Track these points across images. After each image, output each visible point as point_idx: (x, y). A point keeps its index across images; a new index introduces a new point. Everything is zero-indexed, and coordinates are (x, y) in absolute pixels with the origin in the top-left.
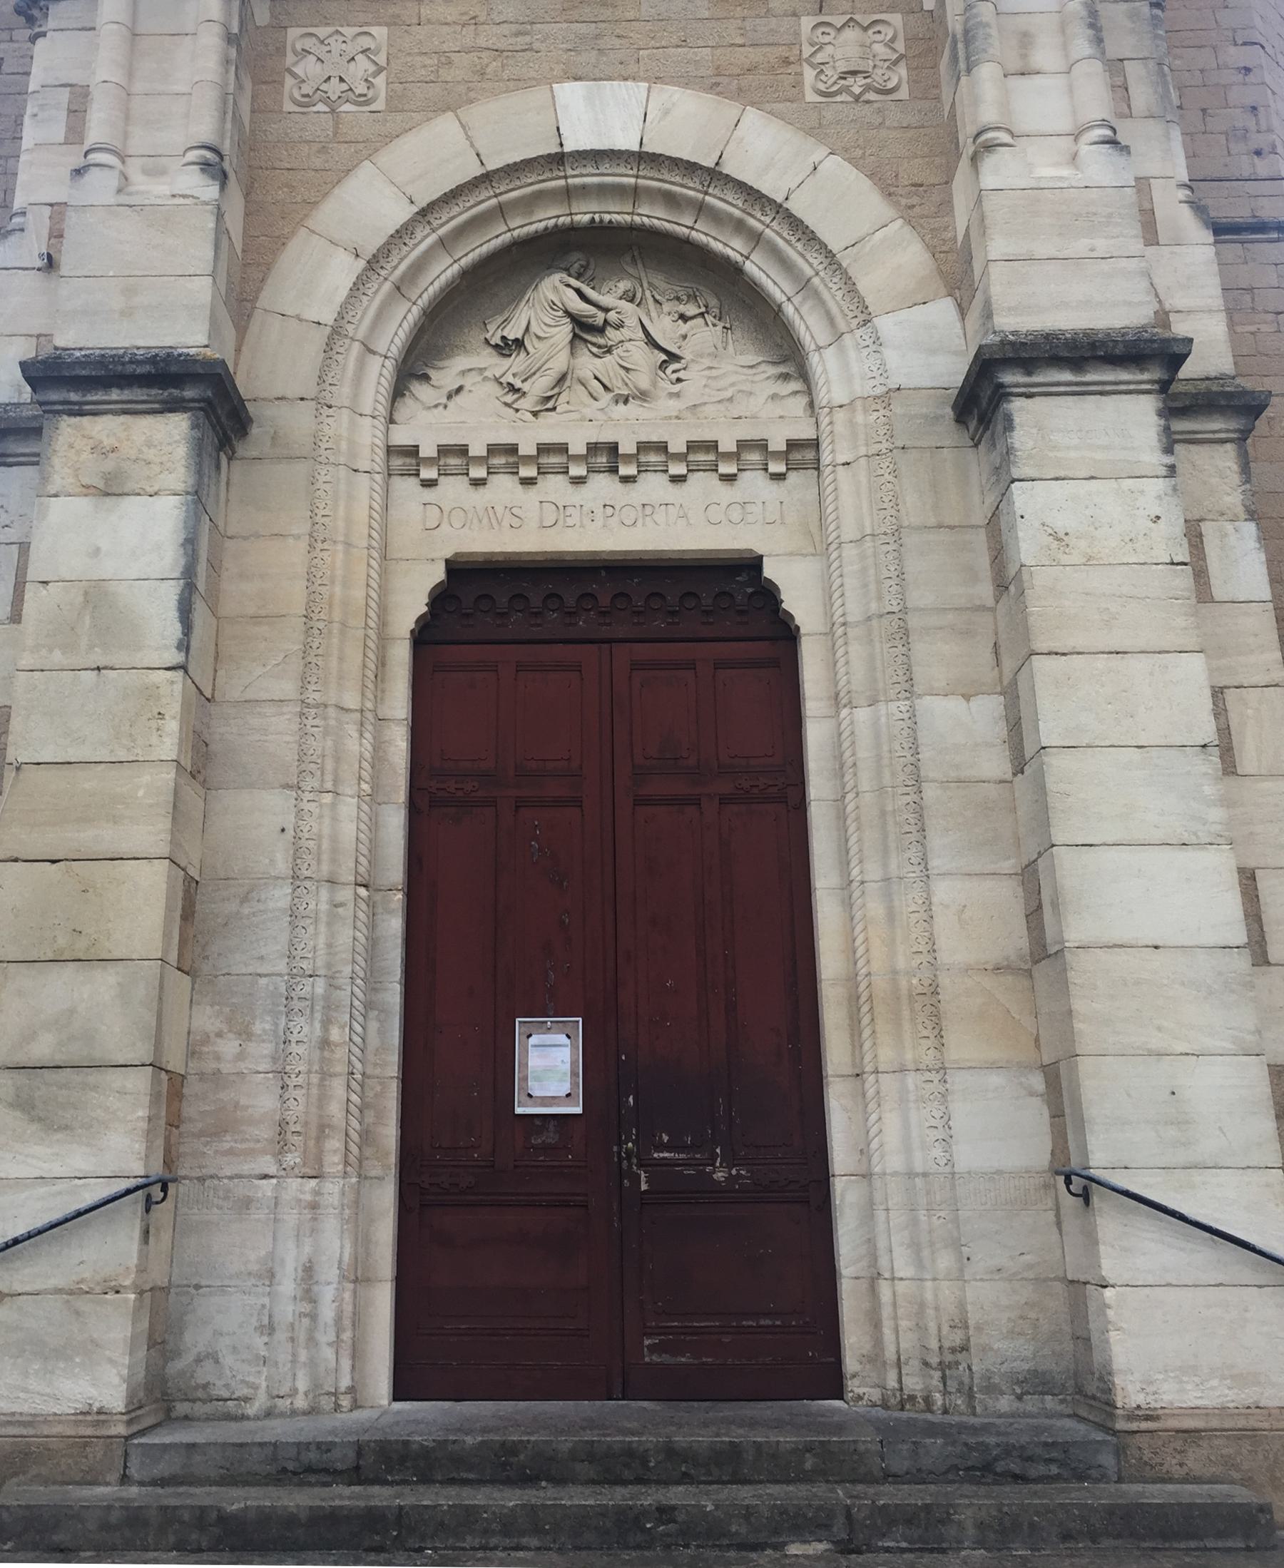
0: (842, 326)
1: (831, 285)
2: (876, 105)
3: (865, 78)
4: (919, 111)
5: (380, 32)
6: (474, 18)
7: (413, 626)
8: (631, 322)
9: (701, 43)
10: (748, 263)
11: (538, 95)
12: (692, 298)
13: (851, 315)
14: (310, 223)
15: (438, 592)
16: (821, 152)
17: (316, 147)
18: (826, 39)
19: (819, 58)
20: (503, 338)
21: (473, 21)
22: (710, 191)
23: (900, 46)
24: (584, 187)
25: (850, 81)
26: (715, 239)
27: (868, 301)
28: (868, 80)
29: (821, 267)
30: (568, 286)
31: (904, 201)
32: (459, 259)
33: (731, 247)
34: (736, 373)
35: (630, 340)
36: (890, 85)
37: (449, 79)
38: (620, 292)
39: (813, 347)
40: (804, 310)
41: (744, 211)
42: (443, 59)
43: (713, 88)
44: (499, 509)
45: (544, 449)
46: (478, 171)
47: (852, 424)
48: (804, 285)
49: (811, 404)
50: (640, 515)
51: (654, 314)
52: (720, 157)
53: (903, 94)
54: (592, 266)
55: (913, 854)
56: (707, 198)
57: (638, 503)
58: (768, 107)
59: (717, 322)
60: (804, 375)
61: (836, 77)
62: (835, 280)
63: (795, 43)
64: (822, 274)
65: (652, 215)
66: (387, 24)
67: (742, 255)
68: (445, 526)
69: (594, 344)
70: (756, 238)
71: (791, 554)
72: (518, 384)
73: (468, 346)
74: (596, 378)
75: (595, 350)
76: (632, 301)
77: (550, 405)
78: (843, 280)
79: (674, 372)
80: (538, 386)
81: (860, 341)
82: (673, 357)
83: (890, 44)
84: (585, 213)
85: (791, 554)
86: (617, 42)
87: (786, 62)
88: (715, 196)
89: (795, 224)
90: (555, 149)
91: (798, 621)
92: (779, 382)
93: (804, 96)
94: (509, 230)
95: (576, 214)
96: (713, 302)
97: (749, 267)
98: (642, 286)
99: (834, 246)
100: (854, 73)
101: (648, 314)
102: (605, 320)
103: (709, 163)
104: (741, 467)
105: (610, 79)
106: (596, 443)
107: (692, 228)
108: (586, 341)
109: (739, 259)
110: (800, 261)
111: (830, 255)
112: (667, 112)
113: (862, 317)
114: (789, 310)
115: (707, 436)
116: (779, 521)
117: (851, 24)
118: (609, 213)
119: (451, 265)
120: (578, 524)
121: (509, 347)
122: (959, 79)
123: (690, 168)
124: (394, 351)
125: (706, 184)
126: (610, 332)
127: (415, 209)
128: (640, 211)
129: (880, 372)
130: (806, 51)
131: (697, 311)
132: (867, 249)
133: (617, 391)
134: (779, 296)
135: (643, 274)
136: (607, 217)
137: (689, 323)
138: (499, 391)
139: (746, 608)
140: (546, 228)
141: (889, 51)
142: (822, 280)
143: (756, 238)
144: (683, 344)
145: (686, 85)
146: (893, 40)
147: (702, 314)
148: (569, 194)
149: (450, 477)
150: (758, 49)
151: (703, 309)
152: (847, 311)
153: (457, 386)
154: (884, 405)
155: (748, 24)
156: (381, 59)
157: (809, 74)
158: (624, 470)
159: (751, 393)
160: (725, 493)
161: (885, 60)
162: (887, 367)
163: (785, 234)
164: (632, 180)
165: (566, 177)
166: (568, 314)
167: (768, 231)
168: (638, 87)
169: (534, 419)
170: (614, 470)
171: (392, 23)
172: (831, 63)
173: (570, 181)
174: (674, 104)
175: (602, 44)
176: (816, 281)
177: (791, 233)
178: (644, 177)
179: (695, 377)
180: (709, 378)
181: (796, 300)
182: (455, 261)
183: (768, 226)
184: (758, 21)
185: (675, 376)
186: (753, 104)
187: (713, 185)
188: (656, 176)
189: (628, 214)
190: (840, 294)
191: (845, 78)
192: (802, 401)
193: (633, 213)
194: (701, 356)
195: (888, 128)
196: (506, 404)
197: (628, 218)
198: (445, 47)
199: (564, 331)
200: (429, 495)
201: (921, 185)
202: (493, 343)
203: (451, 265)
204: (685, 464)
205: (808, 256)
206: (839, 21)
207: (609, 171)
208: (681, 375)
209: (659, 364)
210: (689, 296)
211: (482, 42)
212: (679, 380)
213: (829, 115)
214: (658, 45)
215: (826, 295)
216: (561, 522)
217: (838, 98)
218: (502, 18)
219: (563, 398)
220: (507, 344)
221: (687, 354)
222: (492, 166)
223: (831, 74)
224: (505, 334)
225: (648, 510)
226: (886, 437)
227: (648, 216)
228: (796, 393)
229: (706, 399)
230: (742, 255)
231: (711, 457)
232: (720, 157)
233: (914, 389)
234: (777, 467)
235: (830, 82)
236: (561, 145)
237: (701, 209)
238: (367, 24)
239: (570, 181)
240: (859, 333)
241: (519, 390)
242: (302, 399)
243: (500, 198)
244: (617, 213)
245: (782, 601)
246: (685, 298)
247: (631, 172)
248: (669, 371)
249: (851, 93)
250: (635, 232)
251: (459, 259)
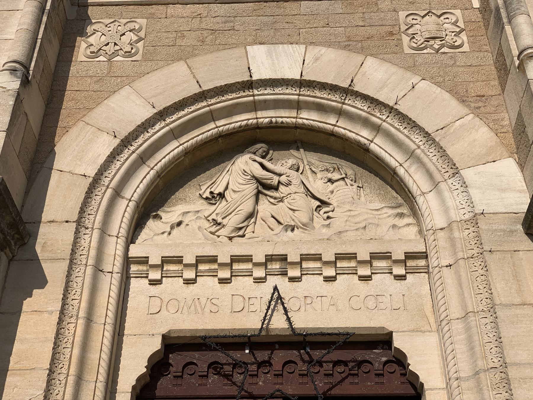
0: (438, 177)
1: (428, 153)
2: (449, 55)
3: (441, 41)
4: (477, 57)
5: (143, 22)
6: (200, 14)
7: (134, 383)
8: (295, 181)
9: (338, 25)
10: (372, 144)
11: (239, 51)
12: (337, 169)
13: (444, 171)
14: (86, 119)
15: (157, 359)
16: (415, 79)
17: (95, 79)
18: (415, 22)
20: (211, 193)
21: (199, 16)
22: (346, 101)
23: (461, 24)
24: (265, 101)
25: (432, 42)
26: (350, 131)
27: (455, 160)
28: (443, 42)
29: (421, 143)
30: (255, 161)
31: (473, 105)
32: (183, 144)
34: (367, 213)
35: (295, 193)
36: (456, 44)
37: (183, 44)
38: (289, 165)
39: (419, 193)
40: (412, 170)
41: (368, 113)
42: (179, 34)
43: (345, 48)
44: (203, 300)
45: (236, 259)
46: (197, 90)
47: (452, 241)
48: (411, 155)
49: (420, 232)
50: (303, 303)
51: (311, 179)
52: (352, 81)
53: (466, 48)
54: (271, 152)
56: (344, 106)
57: (301, 296)
58: (381, 56)
59: (353, 183)
60: (415, 212)
61: (422, 40)
62: (431, 150)
64: (422, 147)
66: (147, 18)
67: (368, 140)
68: (164, 312)
69: (271, 197)
70: (377, 129)
71: (413, 331)
72: (219, 220)
73: (188, 199)
74: (273, 217)
75: (272, 200)
76: (297, 170)
77: (241, 233)
78: (437, 150)
79: (325, 213)
80: (233, 221)
81: (451, 186)
82: (324, 203)
83: (455, 24)
84: (266, 118)
85: (413, 331)
86: (287, 26)
88: (349, 105)
89: (403, 118)
90: (246, 78)
91: (422, 379)
92: (397, 219)
93: (403, 50)
94: (217, 127)
95: (260, 118)
96: (350, 172)
97: (373, 147)
98: (303, 163)
99: (429, 130)
100: (434, 38)
101: (307, 178)
102: (279, 182)
103: (345, 85)
104: (373, 272)
105: (282, 43)
106: (272, 255)
107: (335, 125)
108: (266, 195)
109: (366, 142)
110: (407, 141)
111: (427, 135)
112: (317, 59)
113: (451, 171)
114: (401, 171)
115: (349, 249)
116: (402, 308)
117: (430, 14)
118: (282, 117)
119: (178, 147)
120: (259, 310)
122: (503, 28)
123: (334, 88)
124: (136, 196)
125: (343, 98)
126: (282, 188)
127: (155, 111)
128: (301, 116)
129: (468, 204)
130: (403, 28)
131: (340, 177)
132: (452, 131)
133: (286, 224)
134: (393, 163)
135: (304, 156)
136: (280, 120)
137: (335, 184)
138: (207, 225)
139: (381, 372)
140: (240, 127)
141: (455, 27)
142: (423, 151)
143: (377, 129)
144: (331, 196)
146: (457, 21)
147: (343, 179)
148: (255, 106)
149: (170, 279)
150: (374, 28)
151: (344, 176)
152: (440, 169)
153: (178, 221)
154: (473, 225)
155: (366, 16)
156: (142, 34)
157: (406, 39)
159: (378, 225)
160: (363, 288)
161: (453, 32)
162: (473, 200)
163: (396, 125)
164: (296, 97)
165: (253, 96)
166: (254, 177)
167: (384, 124)
168: (299, 47)
169: (230, 241)
170: (284, 274)
171: (150, 17)
172: (420, 34)
173: (256, 98)
174: (321, 55)
175: (277, 26)
176: (418, 151)
177: (400, 124)
178: (304, 95)
180: (349, 216)
181: (406, 165)
182: (181, 145)
183: (384, 121)
184: (372, 14)
185: (326, 215)
186: (372, 55)
187: (348, 99)
188: (311, 94)
189: (294, 118)
190: (435, 159)
191: (428, 41)
192: (414, 229)
193: (296, 118)
194: (343, 203)
195: (458, 66)
196: (212, 233)
197: (294, 120)
198: (181, 29)
199: (251, 188)
200: (155, 290)
201: (483, 96)
202: (204, 196)
203: (178, 147)
204: (334, 269)
205: (412, 137)
207: (281, 92)
208: (330, 214)
209: (314, 208)
210: (334, 169)
211: (203, 26)
212: (328, 218)
213: (420, 60)
214: (312, 26)
215: (425, 160)
216: (246, 309)
217: (425, 51)
218: (216, 14)
219: (249, 229)
220: (213, 197)
221: (334, 201)
222: (205, 87)
223: (420, 39)
224: (212, 190)
225: (309, 301)
226: (477, 245)
227: (307, 119)
228: (408, 225)
229: (347, 228)
230: (368, 140)
231: (353, 264)
232: (352, 81)
233: (493, 213)
234: (399, 270)
235: (419, 43)
236: (251, 76)
237: (340, 113)
238: (137, 18)
239: (256, 98)
240: (450, 181)
241: (219, 224)
242: (67, 222)
243: (211, 107)
245: (409, 365)
246: (332, 169)
247: (295, 92)
248: (322, 212)
249: (434, 49)
250: (298, 130)
251: (183, 144)
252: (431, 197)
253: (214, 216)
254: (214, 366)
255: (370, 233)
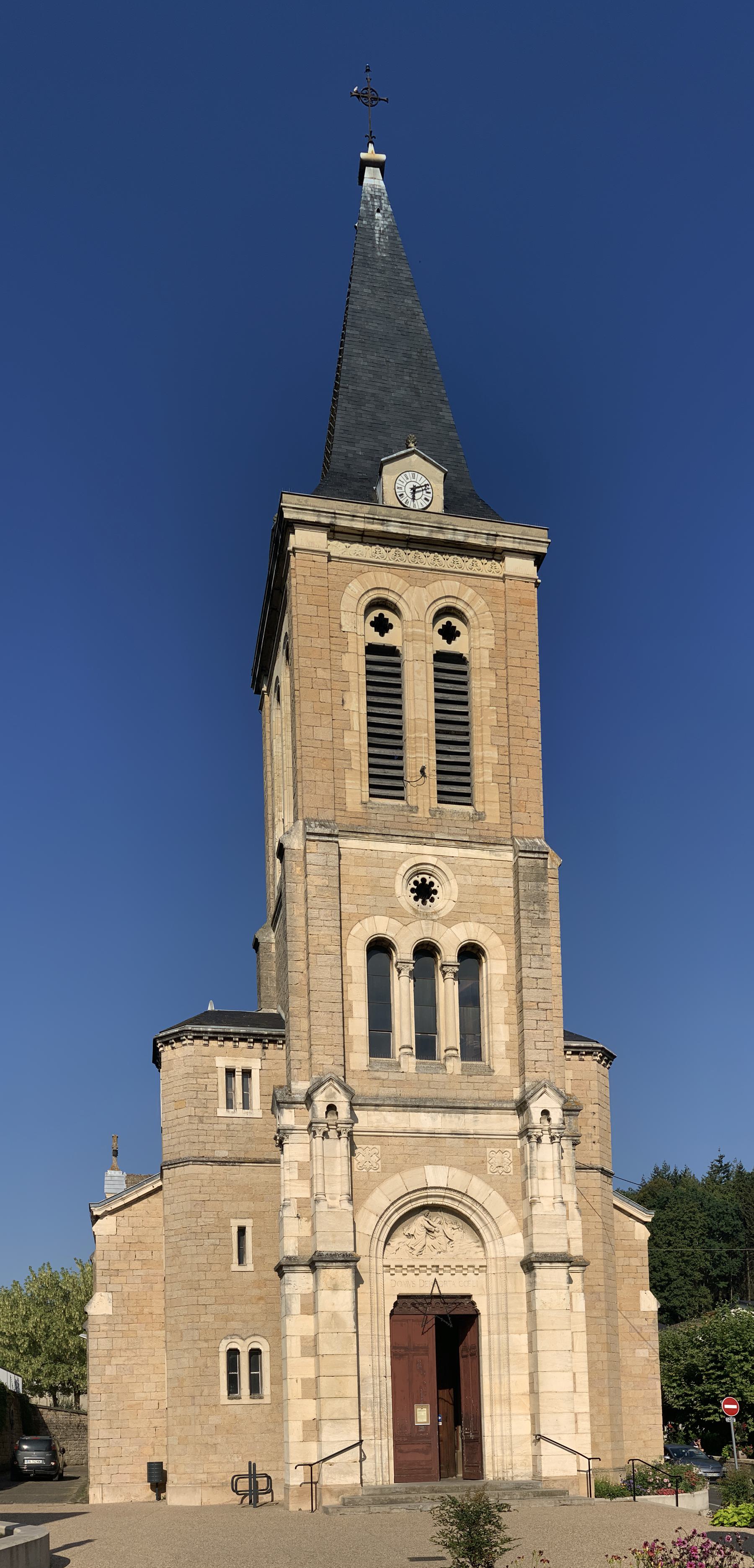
19: (491, 1162)
33: (467, 1212)
55: (506, 1369)
63: (485, 1156)
65: (447, 1203)
87: (483, 1162)
114: (481, 1231)
121: (410, 1236)
130: (488, 1159)
145: (458, 1168)
157: (489, 1166)
158: (441, 1272)
179: (456, 1244)
206: (497, 1150)
231: (461, 1269)
234: (476, 1272)
244: (439, 1201)
252: (491, 1243)
253: (410, 1246)
254: (413, 1305)
255: (467, 1256)
